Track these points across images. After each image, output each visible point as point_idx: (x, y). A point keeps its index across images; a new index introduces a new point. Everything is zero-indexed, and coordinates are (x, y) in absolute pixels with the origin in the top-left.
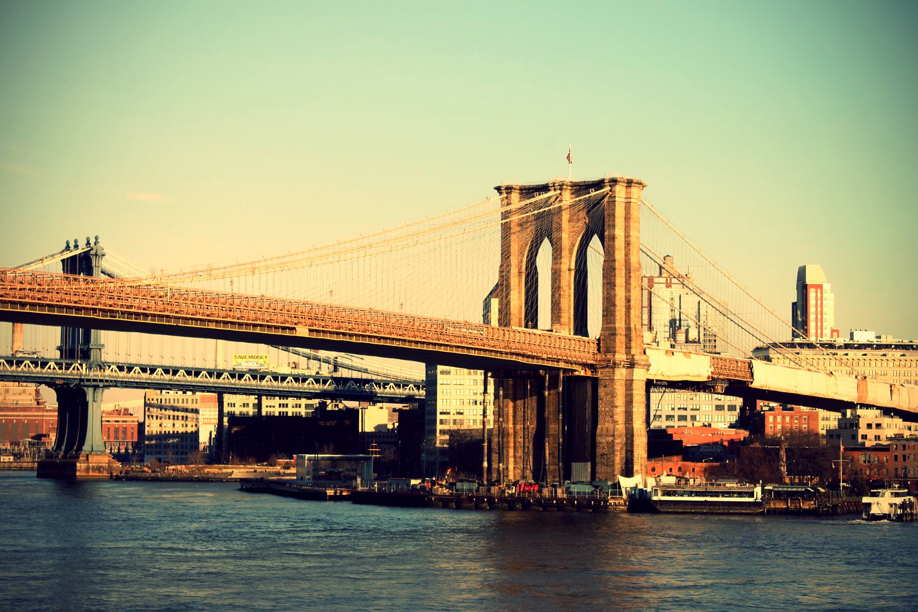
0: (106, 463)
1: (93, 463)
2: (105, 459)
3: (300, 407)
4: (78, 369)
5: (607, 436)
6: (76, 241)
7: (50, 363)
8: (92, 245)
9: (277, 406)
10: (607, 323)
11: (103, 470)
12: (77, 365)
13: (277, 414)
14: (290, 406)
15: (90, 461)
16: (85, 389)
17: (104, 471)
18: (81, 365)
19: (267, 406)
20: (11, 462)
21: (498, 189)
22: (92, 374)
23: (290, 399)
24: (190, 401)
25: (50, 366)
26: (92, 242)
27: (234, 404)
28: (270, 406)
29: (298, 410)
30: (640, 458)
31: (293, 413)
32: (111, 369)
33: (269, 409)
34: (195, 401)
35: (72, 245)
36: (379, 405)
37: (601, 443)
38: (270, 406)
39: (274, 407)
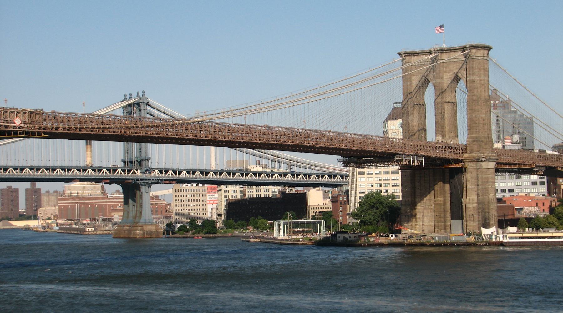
1: (146, 230)
3: (269, 191)
4: (135, 173)
5: (473, 203)
6: (131, 95)
7: (118, 170)
8: (141, 96)
9: (255, 191)
10: (471, 134)
11: (153, 234)
12: (135, 170)
13: (255, 196)
14: (262, 191)
18: (137, 170)
19: (248, 192)
20: (93, 231)
21: (399, 54)
22: (144, 176)
23: (262, 187)
24: (201, 190)
25: (118, 172)
26: (141, 95)
27: (228, 191)
28: (250, 192)
29: (267, 193)
30: (493, 216)
31: (264, 195)
32: (155, 172)
33: (250, 194)
34: (204, 190)
35: (128, 97)
36: (317, 188)
37: (470, 208)
38: (250, 192)
39: (253, 192)
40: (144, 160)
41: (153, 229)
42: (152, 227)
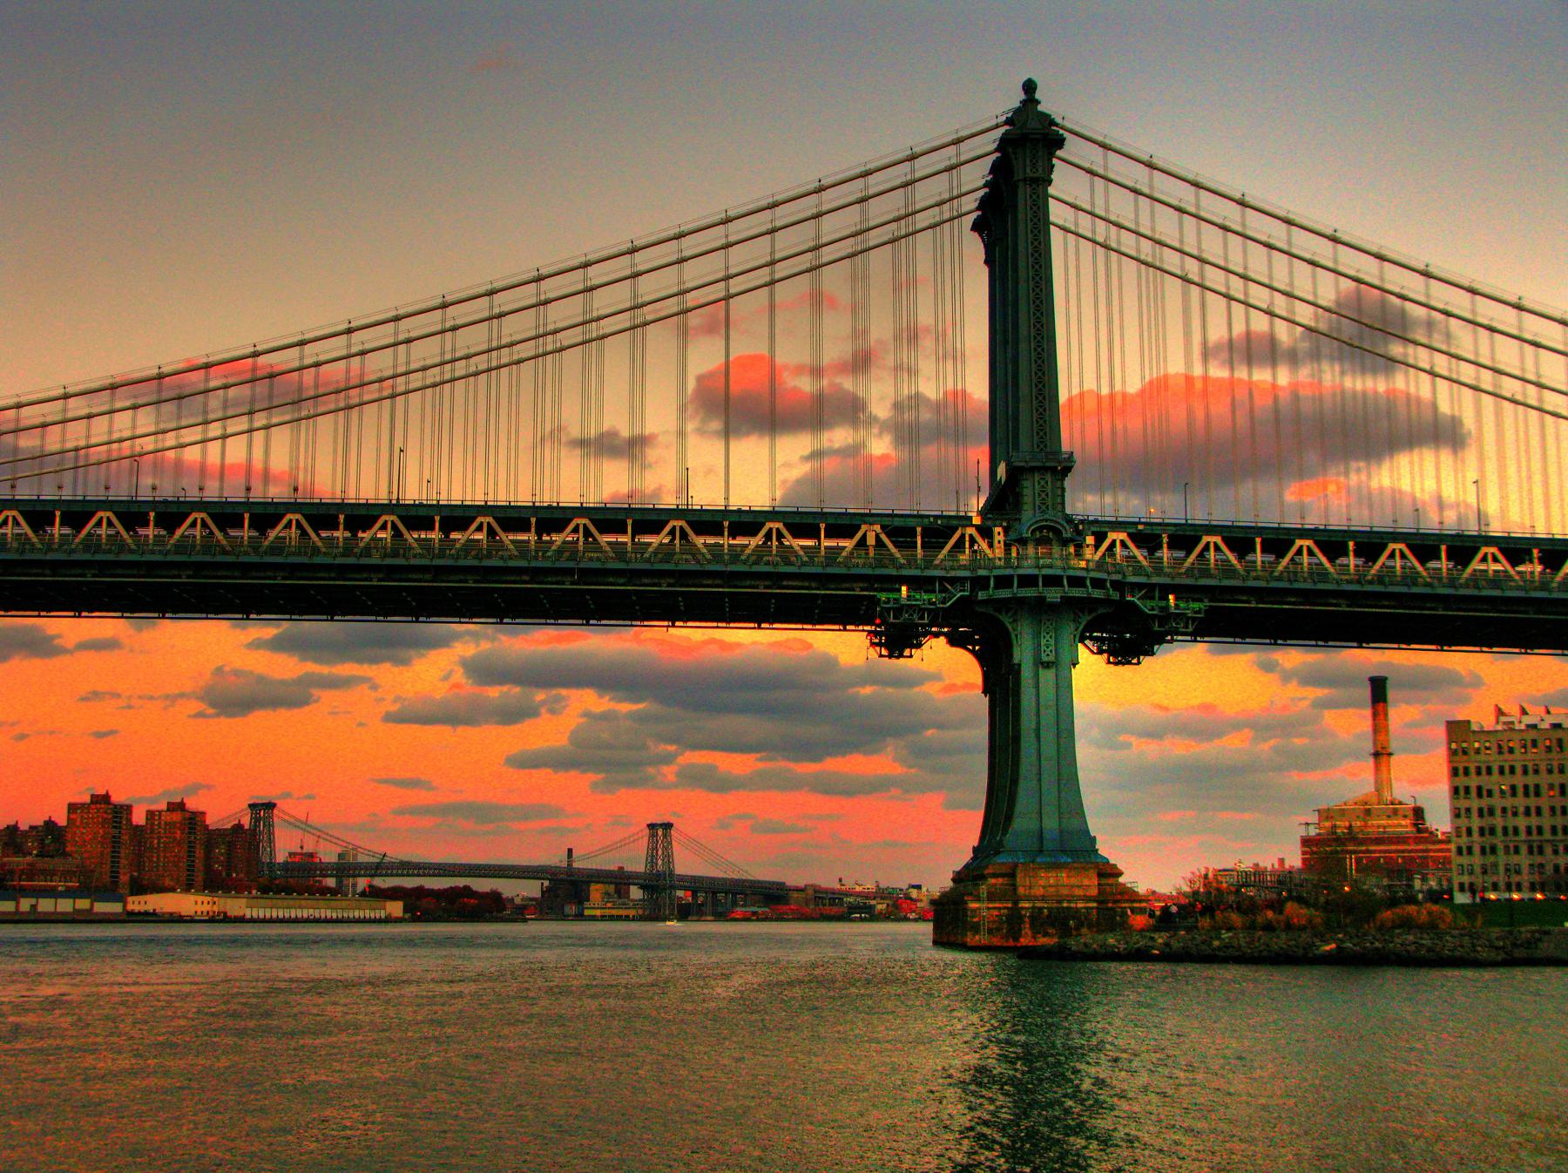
0: (1087, 899)
1: (1028, 898)
2: (1086, 882)
7: (864, 528)
15: (1021, 891)
16: (1006, 620)
40: (1032, 470)
41: (1079, 892)
42: (1074, 881)
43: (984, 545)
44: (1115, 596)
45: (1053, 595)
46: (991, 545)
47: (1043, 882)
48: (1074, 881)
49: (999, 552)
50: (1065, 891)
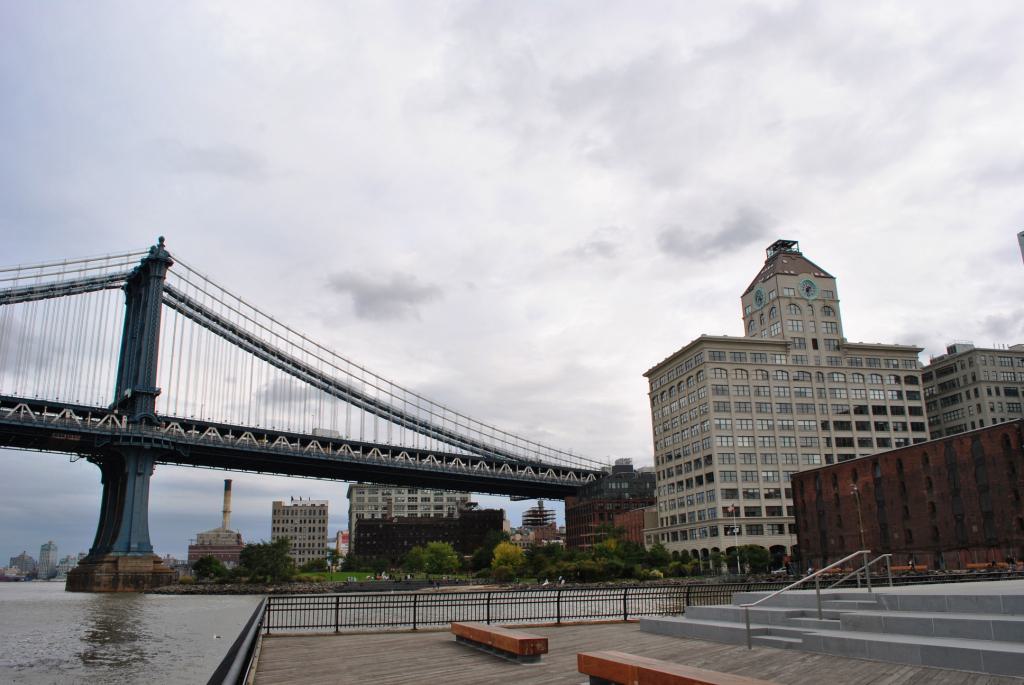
4: (114, 422)
11: (144, 582)
15: (120, 568)
17: (146, 585)
18: (120, 418)
41: (146, 569)
43: (117, 422)
44: (172, 448)
45: (147, 446)
46: (121, 422)
47: (129, 565)
48: (143, 565)
49: (124, 426)
50: (137, 568)
